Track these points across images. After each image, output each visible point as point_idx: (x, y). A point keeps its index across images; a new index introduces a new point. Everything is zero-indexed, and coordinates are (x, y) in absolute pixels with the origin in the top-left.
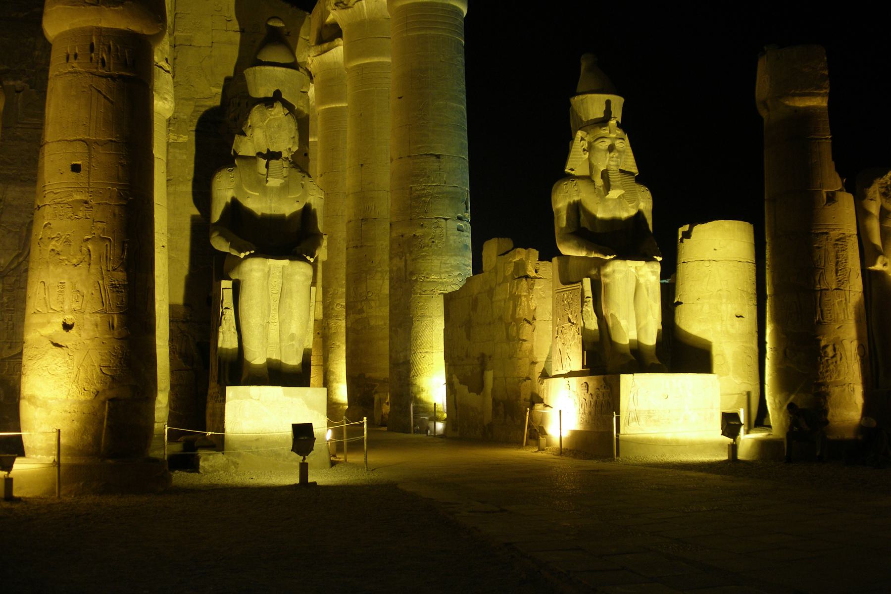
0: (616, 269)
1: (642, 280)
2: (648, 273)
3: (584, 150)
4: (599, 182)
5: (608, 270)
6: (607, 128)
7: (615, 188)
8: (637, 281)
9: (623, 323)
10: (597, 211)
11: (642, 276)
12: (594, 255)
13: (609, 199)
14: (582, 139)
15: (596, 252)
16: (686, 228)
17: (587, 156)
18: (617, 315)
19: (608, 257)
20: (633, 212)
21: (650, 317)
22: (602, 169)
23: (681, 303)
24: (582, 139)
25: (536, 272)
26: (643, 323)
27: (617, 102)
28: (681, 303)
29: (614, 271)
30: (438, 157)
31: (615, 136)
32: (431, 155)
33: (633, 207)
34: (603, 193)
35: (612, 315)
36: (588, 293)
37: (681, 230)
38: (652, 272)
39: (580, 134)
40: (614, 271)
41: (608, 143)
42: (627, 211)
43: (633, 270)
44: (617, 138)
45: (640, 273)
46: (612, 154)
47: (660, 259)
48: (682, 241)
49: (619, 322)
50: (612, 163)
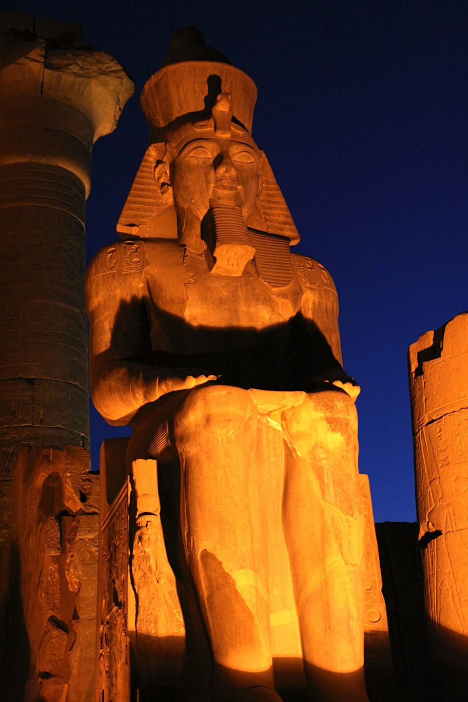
0: (215, 410)
1: (302, 450)
2: (319, 428)
3: (163, 184)
4: (195, 243)
5: (193, 418)
6: (211, 122)
7: (231, 240)
8: (289, 453)
9: (243, 581)
10: (183, 303)
11: (300, 436)
12: (158, 393)
13: (219, 277)
14: (159, 162)
15: (163, 379)
16: (428, 340)
17: (168, 198)
18: (221, 555)
19: (192, 383)
20: (285, 312)
21: (335, 560)
22: (202, 213)
23: (438, 533)
24: (159, 162)
25: (83, 498)
26: (313, 581)
27: (233, 77)
28: (438, 533)
29: (208, 420)
30: (31, 382)
31: (227, 136)
32: (20, 378)
33: (284, 295)
34: (205, 266)
35: (206, 554)
36: (149, 499)
37: (414, 350)
38: (329, 421)
39: (152, 153)
40: (208, 420)
41: (209, 152)
42: (268, 301)
43: (275, 424)
44: (232, 141)
45: (295, 428)
46: (222, 170)
47: (354, 391)
48: (420, 372)
49: (226, 577)
50: (222, 192)
